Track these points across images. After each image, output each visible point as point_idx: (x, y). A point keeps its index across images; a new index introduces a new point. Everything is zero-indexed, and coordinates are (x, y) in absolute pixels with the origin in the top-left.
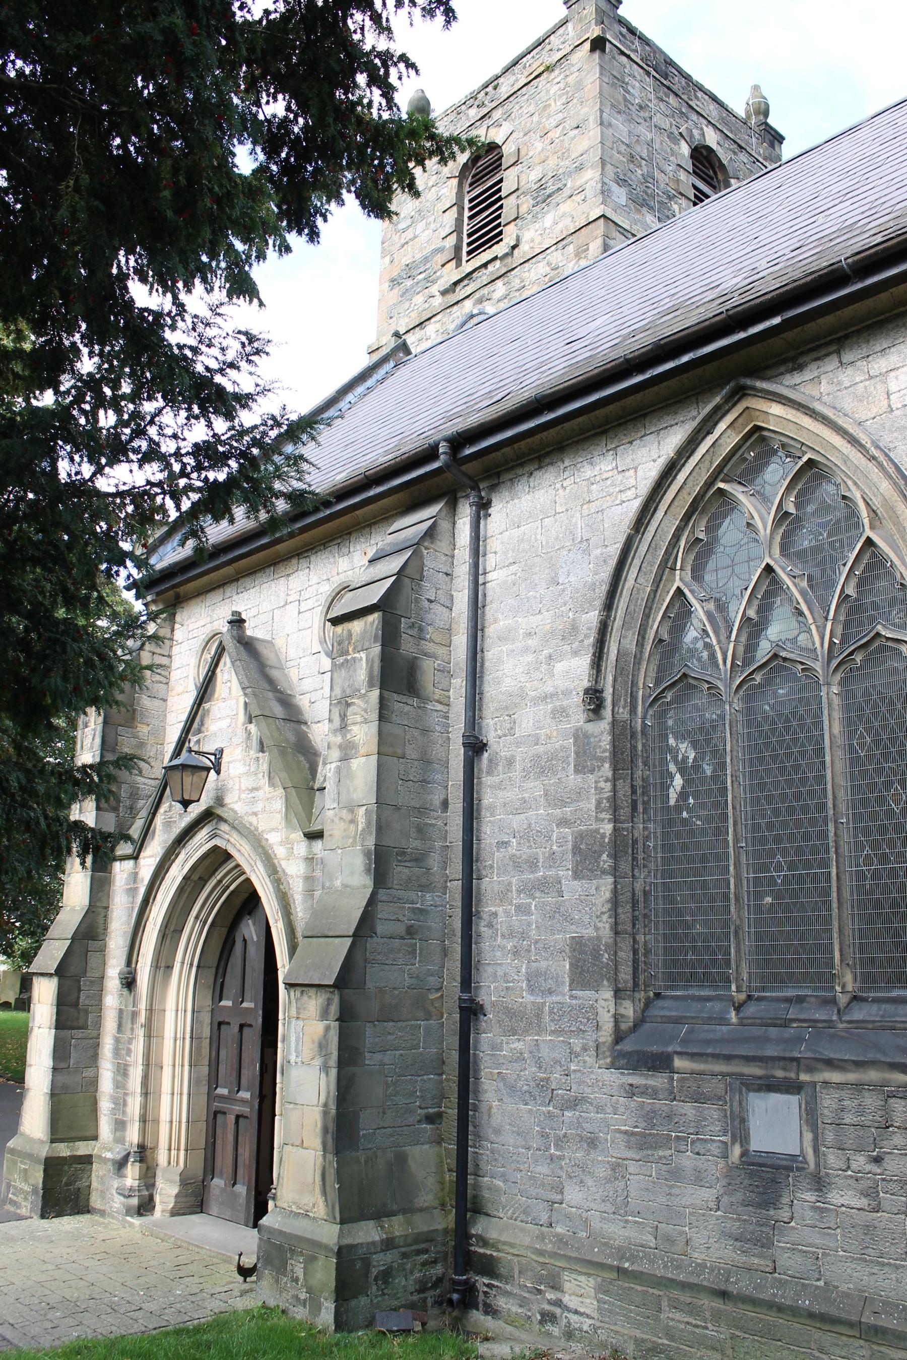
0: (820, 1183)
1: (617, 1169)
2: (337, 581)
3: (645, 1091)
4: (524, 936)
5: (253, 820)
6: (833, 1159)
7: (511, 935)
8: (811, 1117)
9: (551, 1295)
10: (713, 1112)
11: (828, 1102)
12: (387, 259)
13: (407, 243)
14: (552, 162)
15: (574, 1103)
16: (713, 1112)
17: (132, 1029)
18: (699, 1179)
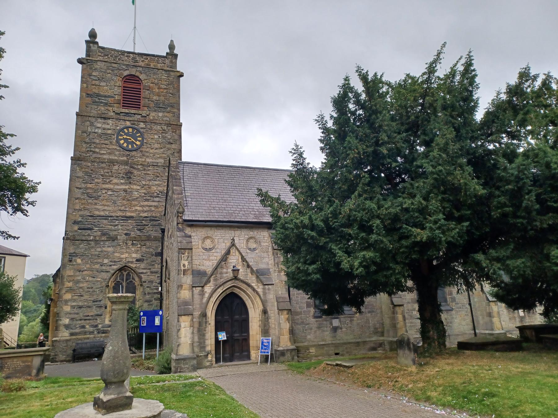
0: (341, 328)
1: (315, 332)
2: (250, 236)
3: (318, 321)
4: (298, 301)
5: (247, 281)
6: (343, 326)
7: (295, 301)
8: (340, 321)
9: (308, 351)
10: (328, 322)
11: (342, 319)
12: (85, 85)
13: (96, 85)
14: (162, 98)
15: (308, 324)
16: (328, 322)
17: (206, 325)
18: (327, 331)
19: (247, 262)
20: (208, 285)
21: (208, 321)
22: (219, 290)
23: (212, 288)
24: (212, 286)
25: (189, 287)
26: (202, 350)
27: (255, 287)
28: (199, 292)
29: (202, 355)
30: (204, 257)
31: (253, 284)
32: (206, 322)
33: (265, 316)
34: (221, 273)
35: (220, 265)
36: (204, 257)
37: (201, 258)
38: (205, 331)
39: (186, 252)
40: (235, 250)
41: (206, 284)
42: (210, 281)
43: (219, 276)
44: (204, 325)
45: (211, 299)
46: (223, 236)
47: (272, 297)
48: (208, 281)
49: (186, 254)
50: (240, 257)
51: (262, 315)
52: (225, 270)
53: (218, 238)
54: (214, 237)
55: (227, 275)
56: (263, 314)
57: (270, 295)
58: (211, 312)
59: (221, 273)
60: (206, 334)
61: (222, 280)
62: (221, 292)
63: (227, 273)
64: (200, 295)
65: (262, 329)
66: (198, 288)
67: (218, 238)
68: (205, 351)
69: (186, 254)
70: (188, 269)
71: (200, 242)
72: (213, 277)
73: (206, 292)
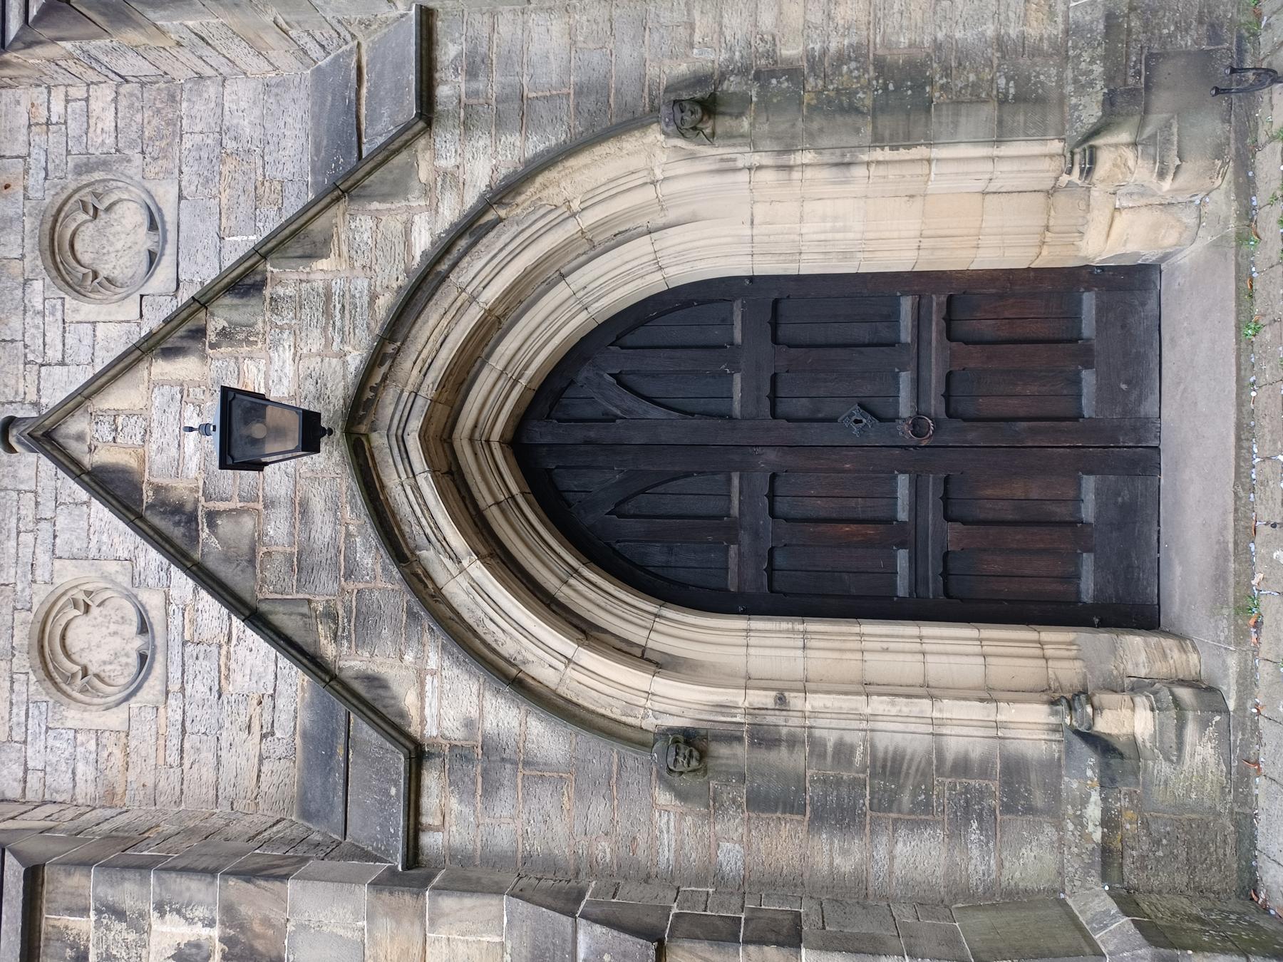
2: (34, 261)
17: (793, 742)
19: (202, 302)
21: (753, 711)
22: (457, 591)
23: (433, 659)
24: (421, 657)
25: (395, 914)
26: (1039, 799)
27: (450, 211)
28: (466, 794)
29: (1094, 811)
30: (199, 689)
31: (422, 241)
32: (764, 738)
33: (741, 104)
34: (301, 564)
35: (228, 573)
36: (199, 689)
37: (202, 717)
38: (843, 752)
39: (61, 934)
40: (95, 418)
42: (375, 681)
43: (323, 591)
44: (781, 758)
45: (544, 672)
46: (28, 511)
47: (558, 26)
49: (84, 925)
50: (161, 368)
51: (730, 136)
52: (278, 529)
53: (43, 558)
54: (40, 595)
55: (317, 505)
56: (723, 124)
57: (535, 48)
58: (662, 685)
59: (301, 564)
60: (884, 742)
63: (302, 509)
64: (491, 788)
65: (878, 141)
66: (431, 801)
67: (43, 558)
68: (1053, 768)
69: (84, 925)
70: (229, 911)
71: (73, 716)
72: (329, 650)
73: (469, 724)
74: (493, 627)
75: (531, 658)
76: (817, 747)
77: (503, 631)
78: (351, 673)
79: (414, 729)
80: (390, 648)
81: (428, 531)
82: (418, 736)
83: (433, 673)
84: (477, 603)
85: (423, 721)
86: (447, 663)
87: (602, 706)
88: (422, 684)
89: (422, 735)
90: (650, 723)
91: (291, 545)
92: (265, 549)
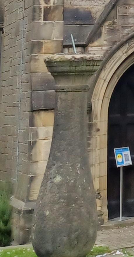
17: (90, 133)
20: (96, 43)
21: (96, 123)
23: (105, 48)
24: (105, 45)
32: (90, 126)
34: (125, 16)
38: (89, 145)
41: (91, 40)
42: (100, 35)
43: (119, 21)
48: (96, 35)
61: (126, 31)
62: (124, 58)
72: (106, 24)
74: (112, 62)
75: (106, 71)
76: (89, 139)
77: (111, 65)
78: (102, 29)
79: (90, 45)
80: (107, 38)
81: (132, 45)
82: (88, 46)
83: (102, 48)
84: (117, 58)
85: (92, 47)
86: (104, 52)
87: (96, 89)
88: (100, 46)
89: (88, 47)
90: (92, 100)
91: (129, 13)
92: (128, 7)
